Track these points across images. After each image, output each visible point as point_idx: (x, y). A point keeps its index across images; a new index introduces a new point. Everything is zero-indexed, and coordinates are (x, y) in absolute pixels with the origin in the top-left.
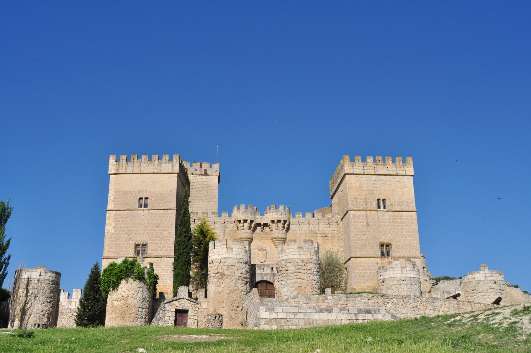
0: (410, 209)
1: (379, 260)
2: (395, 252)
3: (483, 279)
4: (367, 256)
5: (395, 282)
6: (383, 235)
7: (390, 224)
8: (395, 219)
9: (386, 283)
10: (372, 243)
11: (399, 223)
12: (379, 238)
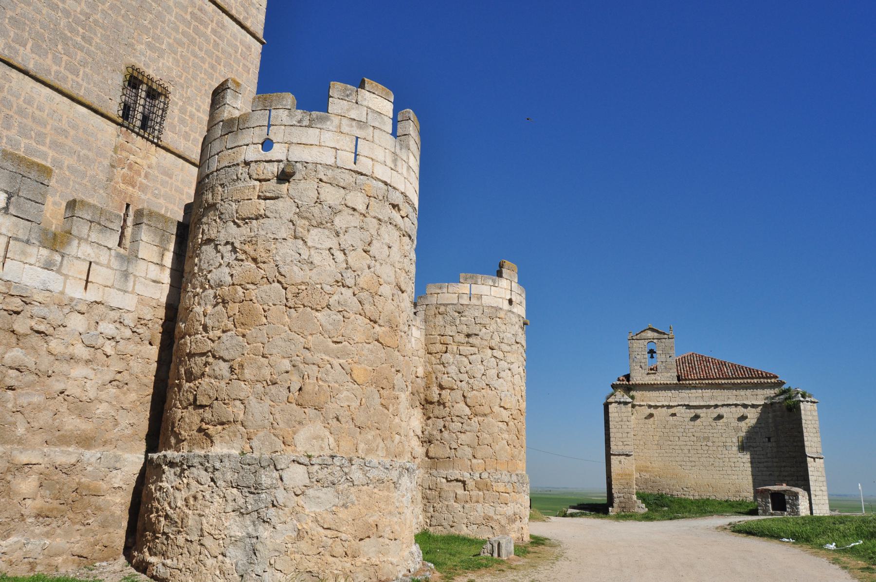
0: (248, 24)
1: (112, 128)
2: (173, 128)
3: (506, 306)
4: (66, 87)
5: (358, 201)
6: (149, 45)
7: (182, 27)
8: (201, 21)
9: (303, 189)
10: (98, 47)
11: (207, 41)
12: (131, 45)
